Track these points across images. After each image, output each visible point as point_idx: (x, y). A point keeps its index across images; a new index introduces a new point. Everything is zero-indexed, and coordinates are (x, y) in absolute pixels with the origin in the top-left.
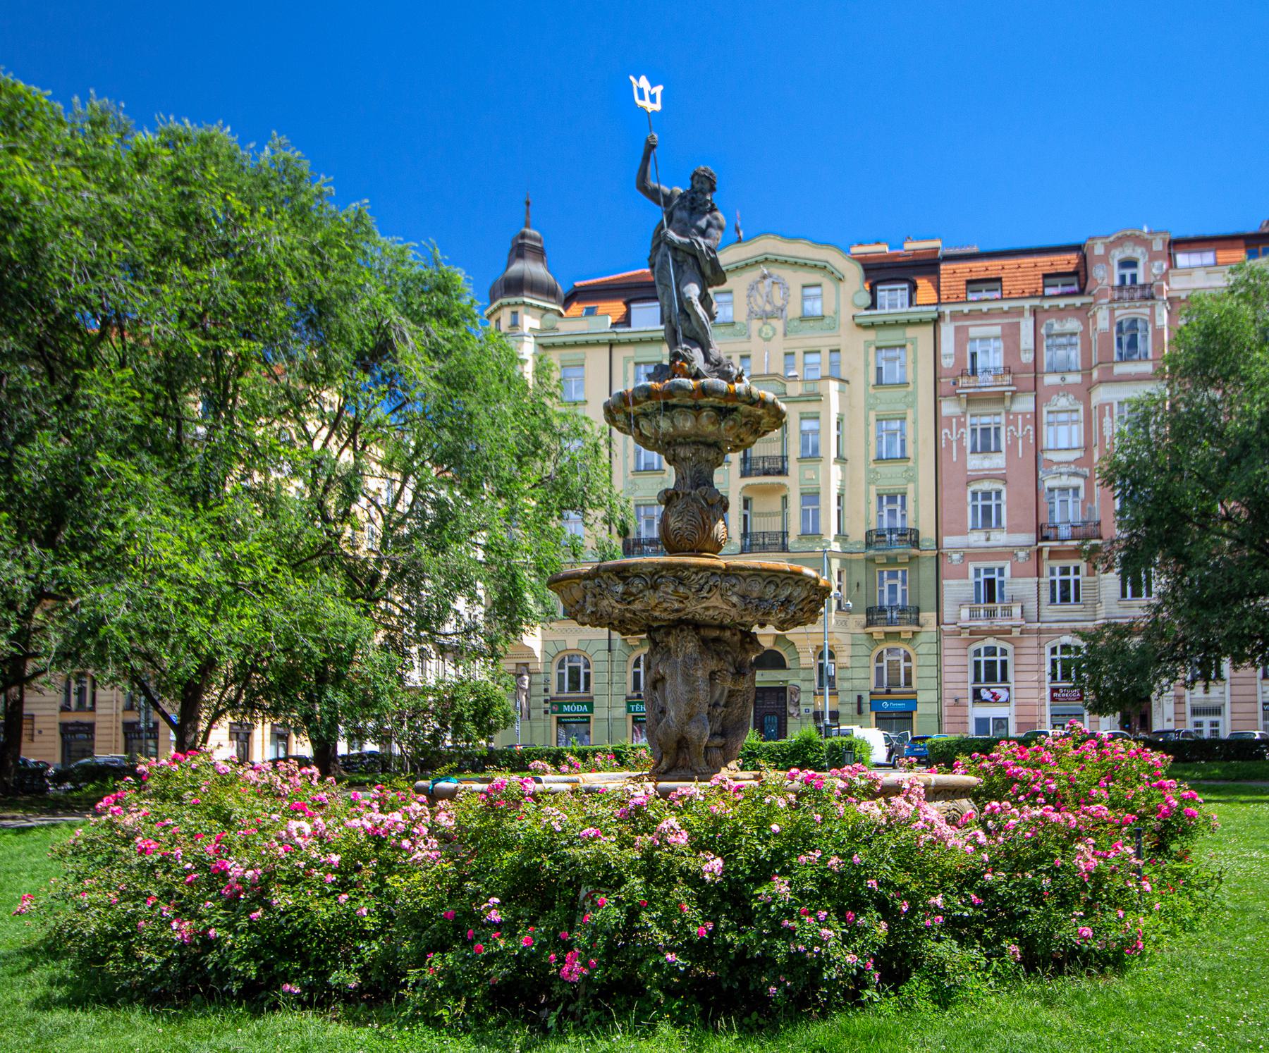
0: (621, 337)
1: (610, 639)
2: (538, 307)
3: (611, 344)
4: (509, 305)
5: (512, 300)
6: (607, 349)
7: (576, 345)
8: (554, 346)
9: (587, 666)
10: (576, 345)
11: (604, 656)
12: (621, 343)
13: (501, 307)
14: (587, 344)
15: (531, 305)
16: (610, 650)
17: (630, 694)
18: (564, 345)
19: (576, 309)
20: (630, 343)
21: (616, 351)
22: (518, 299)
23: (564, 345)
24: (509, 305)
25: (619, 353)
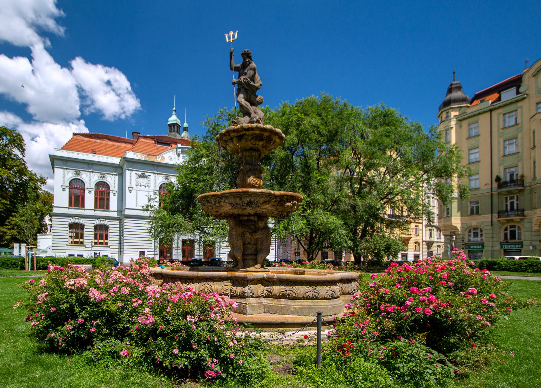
0: (495, 106)
1: (492, 221)
2: (457, 107)
3: (491, 111)
4: (445, 110)
5: (446, 108)
6: (489, 113)
7: (474, 116)
8: (464, 119)
9: (481, 231)
10: (474, 116)
11: (490, 227)
12: (495, 109)
13: (442, 112)
14: (479, 114)
15: (454, 108)
16: (492, 225)
17: (502, 241)
18: (469, 117)
19: (475, 102)
20: (500, 107)
21: (493, 113)
22: (449, 107)
23: (469, 117)
24: (445, 110)
25: (495, 113)
